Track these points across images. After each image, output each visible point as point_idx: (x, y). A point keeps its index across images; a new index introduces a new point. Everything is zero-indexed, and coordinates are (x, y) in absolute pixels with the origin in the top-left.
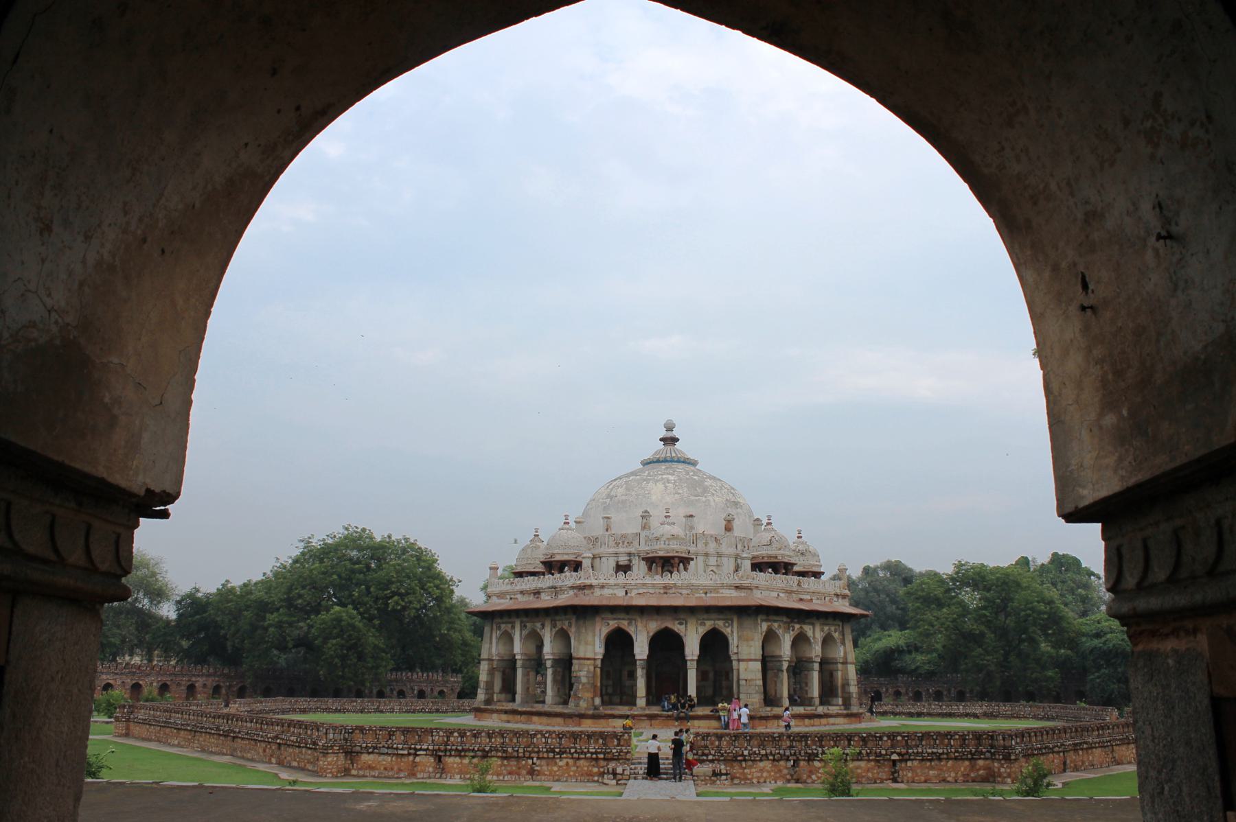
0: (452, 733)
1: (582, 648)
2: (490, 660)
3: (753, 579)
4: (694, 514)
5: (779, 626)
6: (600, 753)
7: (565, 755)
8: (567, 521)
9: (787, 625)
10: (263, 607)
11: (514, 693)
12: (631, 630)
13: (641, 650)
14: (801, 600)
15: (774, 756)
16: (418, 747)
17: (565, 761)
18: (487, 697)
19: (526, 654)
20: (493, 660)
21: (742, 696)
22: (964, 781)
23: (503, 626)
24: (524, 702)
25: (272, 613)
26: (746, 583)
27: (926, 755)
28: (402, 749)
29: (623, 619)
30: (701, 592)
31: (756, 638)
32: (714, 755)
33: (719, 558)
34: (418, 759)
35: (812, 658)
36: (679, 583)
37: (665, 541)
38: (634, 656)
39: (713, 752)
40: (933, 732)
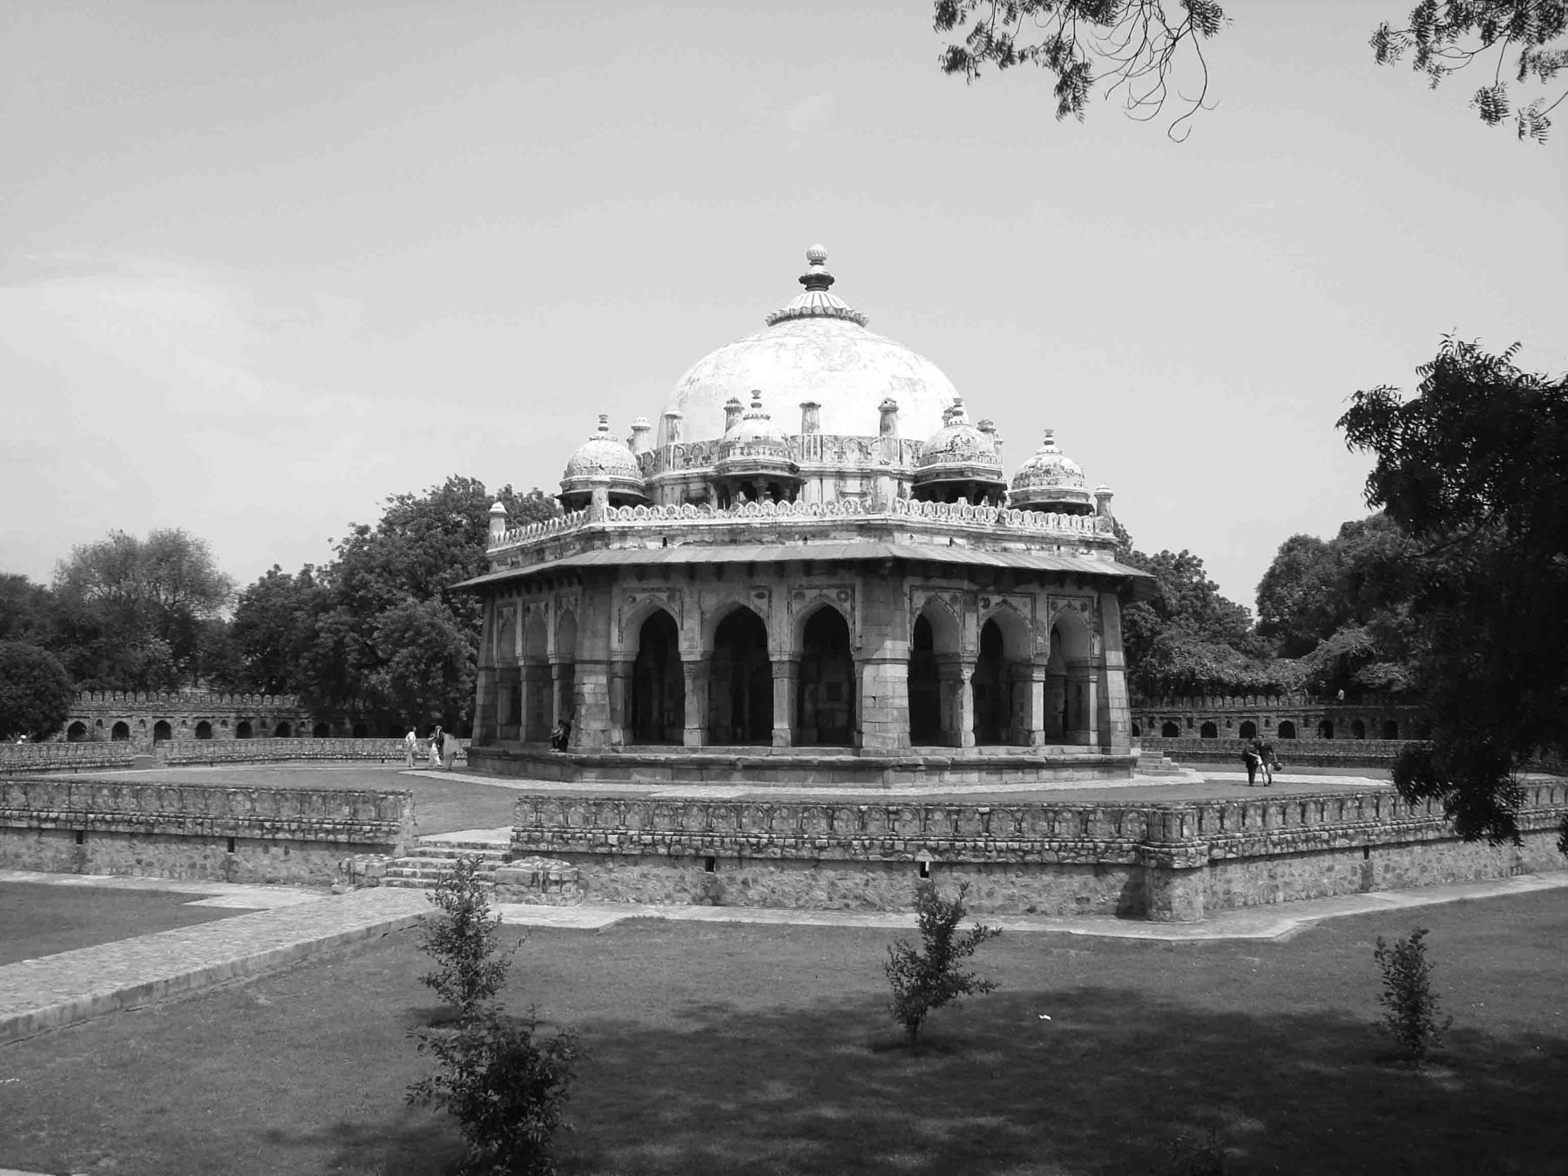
0: (100, 789)
1: (587, 643)
2: (487, 668)
3: (894, 510)
4: (815, 402)
5: (954, 599)
6: (341, 832)
7: (280, 836)
8: (603, 425)
9: (969, 598)
10: (322, 604)
11: (519, 722)
12: (673, 610)
13: (692, 644)
14: (1005, 550)
15: (669, 846)
16: (43, 815)
17: (284, 844)
18: (484, 731)
19: (533, 658)
20: (495, 669)
21: (865, 727)
22: (1079, 913)
23: (505, 610)
24: (533, 738)
25: (327, 612)
26: (876, 517)
27: (994, 853)
28: (19, 819)
29: (659, 590)
30: (797, 537)
31: (898, 620)
32: (552, 843)
33: (864, 482)
34: (44, 839)
35: (1030, 659)
36: (756, 522)
37: (742, 448)
38: (679, 655)
39: (548, 835)
40: (1018, 805)
